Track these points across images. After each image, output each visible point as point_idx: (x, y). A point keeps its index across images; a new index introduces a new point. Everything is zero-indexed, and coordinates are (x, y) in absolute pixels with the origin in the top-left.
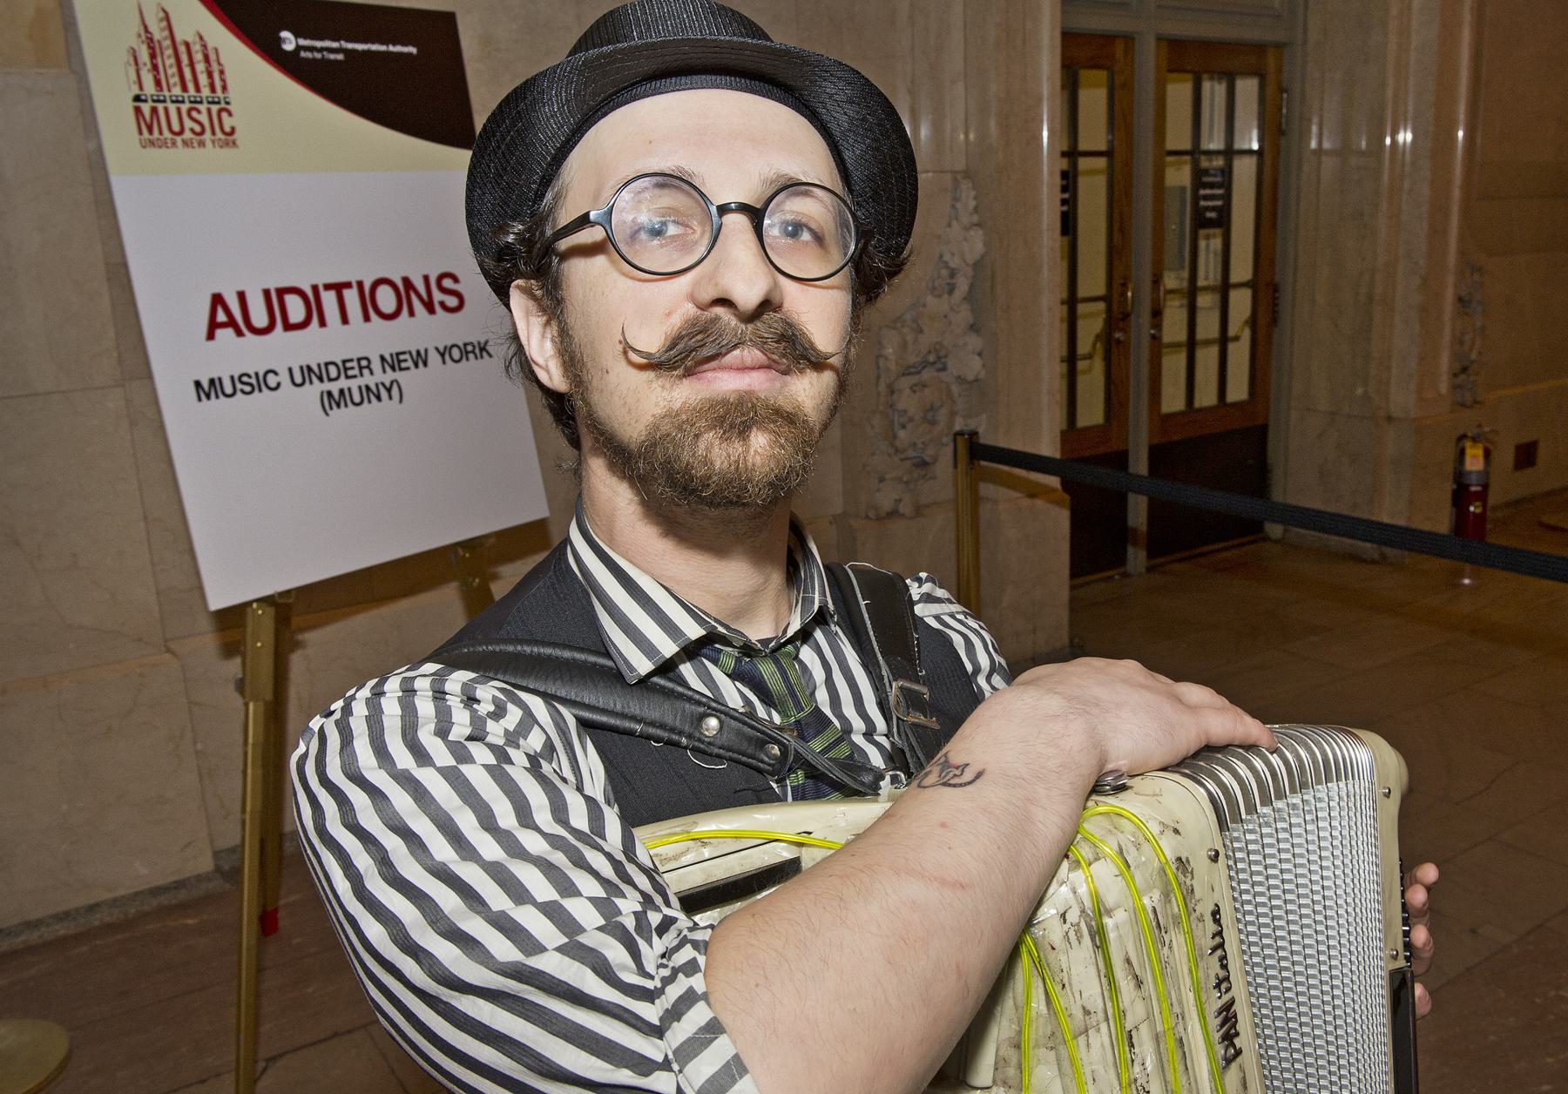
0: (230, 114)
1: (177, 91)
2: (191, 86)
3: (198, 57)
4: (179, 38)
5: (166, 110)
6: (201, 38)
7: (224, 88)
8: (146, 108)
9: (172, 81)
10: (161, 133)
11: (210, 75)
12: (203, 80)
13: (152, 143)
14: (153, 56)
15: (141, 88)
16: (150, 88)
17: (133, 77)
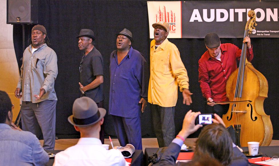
0: (175, 26)
2: (167, 21)
3: (170, 15)
4: (167, 12)
6: (171, 11)
7: (175, 21)
11: (172, 19)
12: (170, 20)
15: (157, 22)
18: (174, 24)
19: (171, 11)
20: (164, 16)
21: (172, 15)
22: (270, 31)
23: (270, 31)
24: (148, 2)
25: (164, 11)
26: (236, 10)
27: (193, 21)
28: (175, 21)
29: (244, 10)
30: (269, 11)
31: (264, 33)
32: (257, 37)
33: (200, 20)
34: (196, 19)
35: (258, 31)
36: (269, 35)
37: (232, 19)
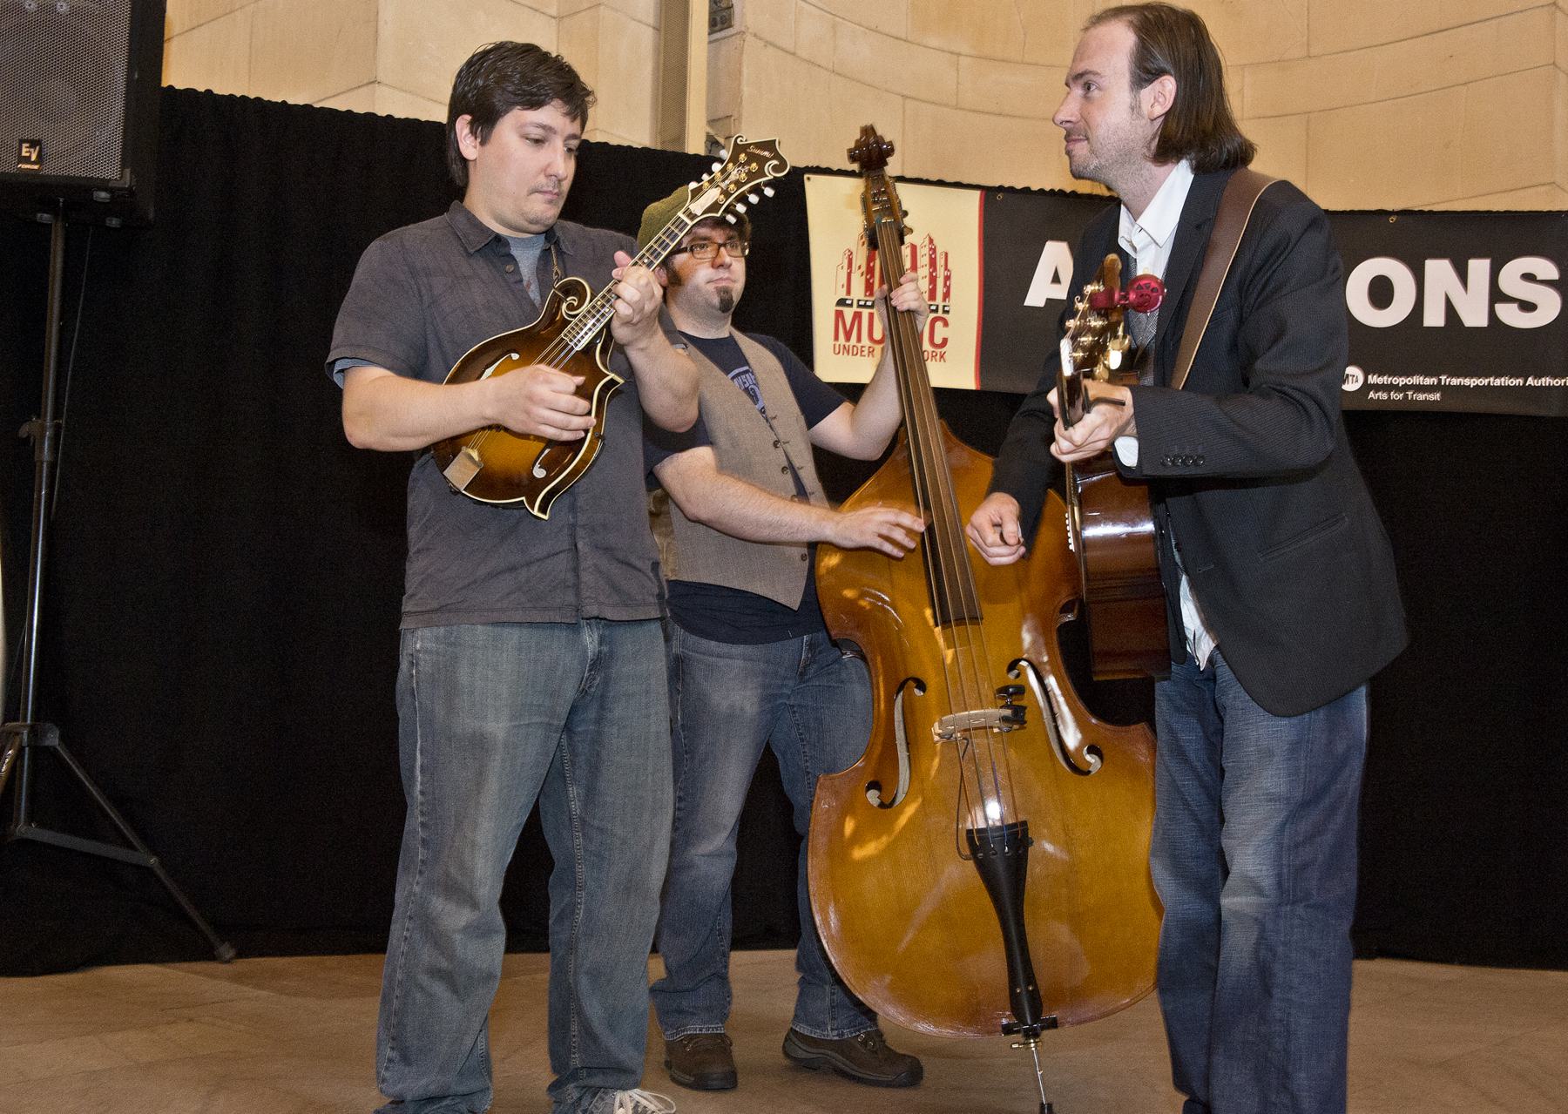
0: (946, 324)
5: (871, 315)
6: (931, 241)
7: (946, 295)
8: (848, 313)
10: (859, 340)
11: (933, 280)
13: (847, 350)
15: (849, 292)
16: (858, 292)
19: (931, 241)
21: (933, 263)
31: (1406, 388)
32: (1370, 408)
35: (1373, 379)
36: (1437, 396)
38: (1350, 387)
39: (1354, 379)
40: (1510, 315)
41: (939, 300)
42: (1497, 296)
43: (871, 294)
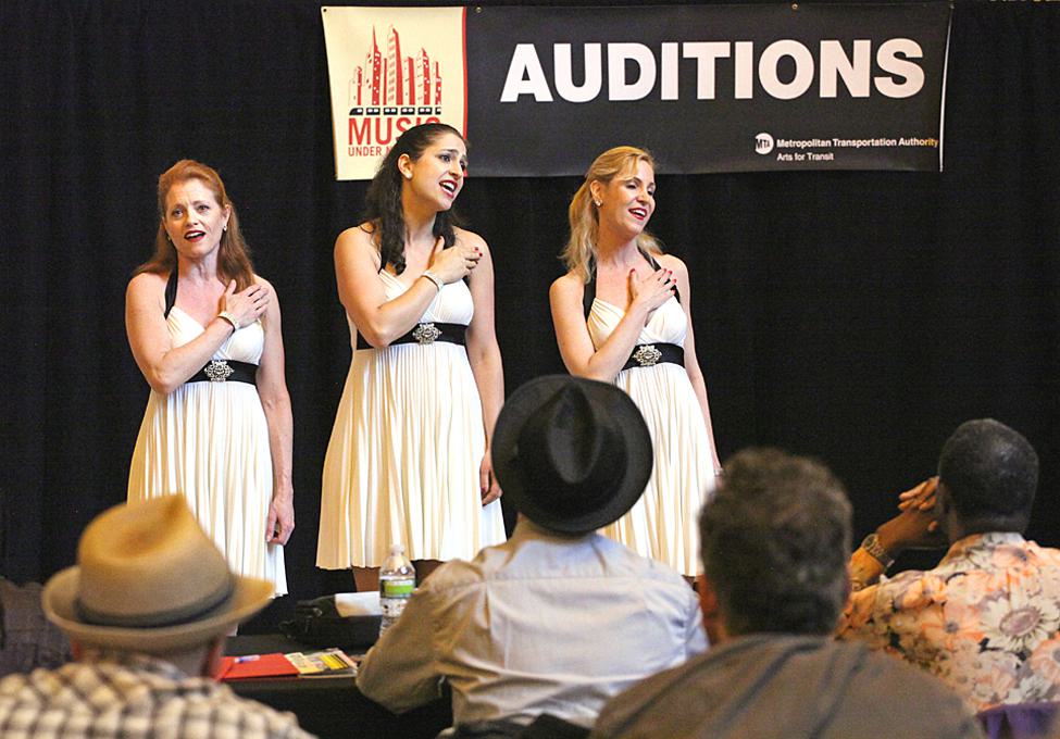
1: (392, 104)
2: (406, 99)
3: (419, 71)
4: (404, 56)
5: (378, 120)
6: (425, 54)
7: (438, 99)
9: (388, 95)
10: (369, 143)
11: (427, 87)
12: (419, 92)
14: (376, 73)
15: (359, 103)
16: (367, 102)
17: (356, 94)
18: (434, 115)
19: (425, 54)
20: (392, 74)
21: (426, 72)
22: (833, 143)
23: (835, 140)
24: (323, 8)
25: (394, 51)
26: (685, 45)
27: (515, 99)
28: (438, 99)
29: (722, 49)
30: (831, 49)
31: (808, 149)
33: (543, 95)
34: (526, 88)
35: (781, 143)
36: (830, 157)
37: (670, 91)
38: (763, 150)
39: (765, 143)
40: (886, 87)
41: (432, 104)
42: (876, 71)
43: (378, 103)
